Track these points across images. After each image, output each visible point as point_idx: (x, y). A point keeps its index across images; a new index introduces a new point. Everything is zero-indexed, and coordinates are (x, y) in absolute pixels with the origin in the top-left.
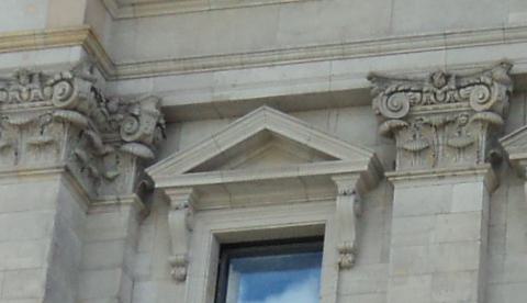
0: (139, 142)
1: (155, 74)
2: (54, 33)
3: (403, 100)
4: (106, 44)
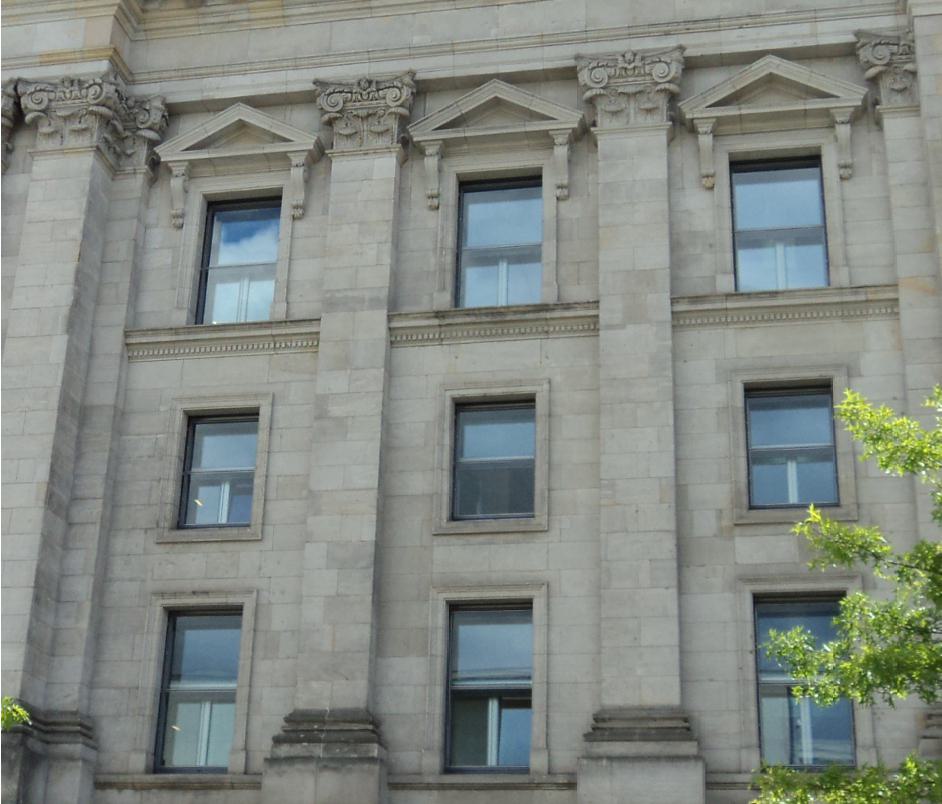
0: (150, 128)
1: (161, 80)
2: (89, 51)
3: (338, 98)
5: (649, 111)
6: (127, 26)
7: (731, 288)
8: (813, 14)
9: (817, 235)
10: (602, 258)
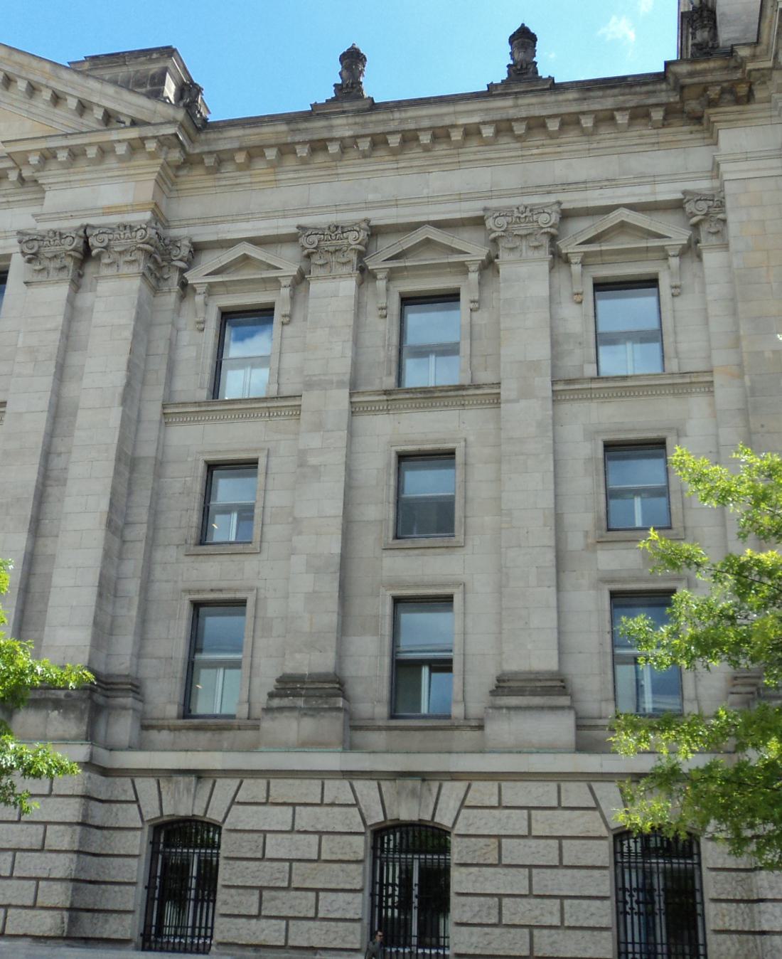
0: (181, 260)
1: (188, 225)
3: (315, 239)
4: (163, 210)
5: (536, 247)
6: (164, 187)
7: (594, 374)
8: (652, 179)
9: (656, 336)
10: (502, 352)
